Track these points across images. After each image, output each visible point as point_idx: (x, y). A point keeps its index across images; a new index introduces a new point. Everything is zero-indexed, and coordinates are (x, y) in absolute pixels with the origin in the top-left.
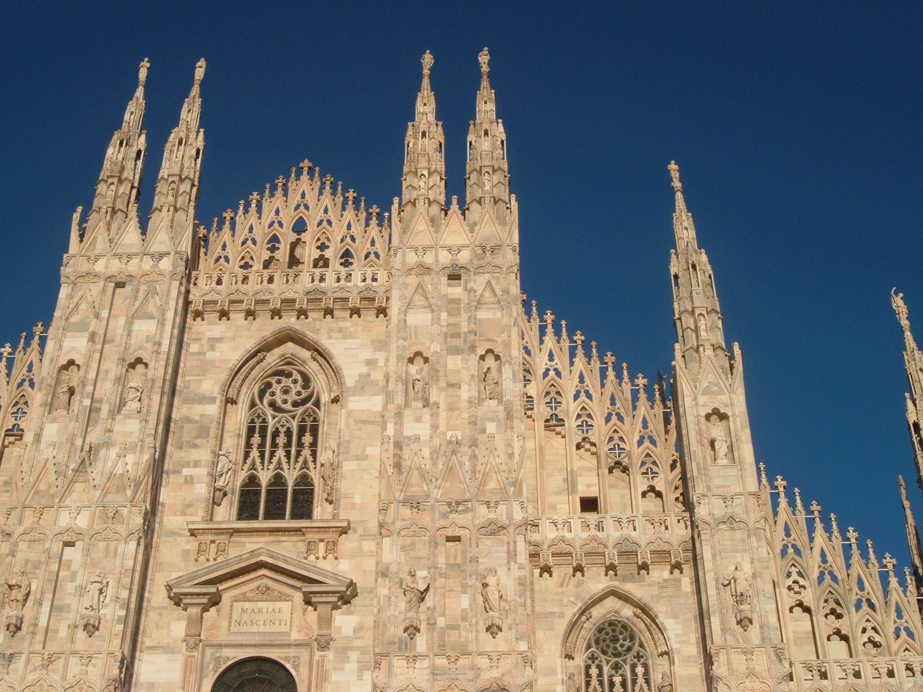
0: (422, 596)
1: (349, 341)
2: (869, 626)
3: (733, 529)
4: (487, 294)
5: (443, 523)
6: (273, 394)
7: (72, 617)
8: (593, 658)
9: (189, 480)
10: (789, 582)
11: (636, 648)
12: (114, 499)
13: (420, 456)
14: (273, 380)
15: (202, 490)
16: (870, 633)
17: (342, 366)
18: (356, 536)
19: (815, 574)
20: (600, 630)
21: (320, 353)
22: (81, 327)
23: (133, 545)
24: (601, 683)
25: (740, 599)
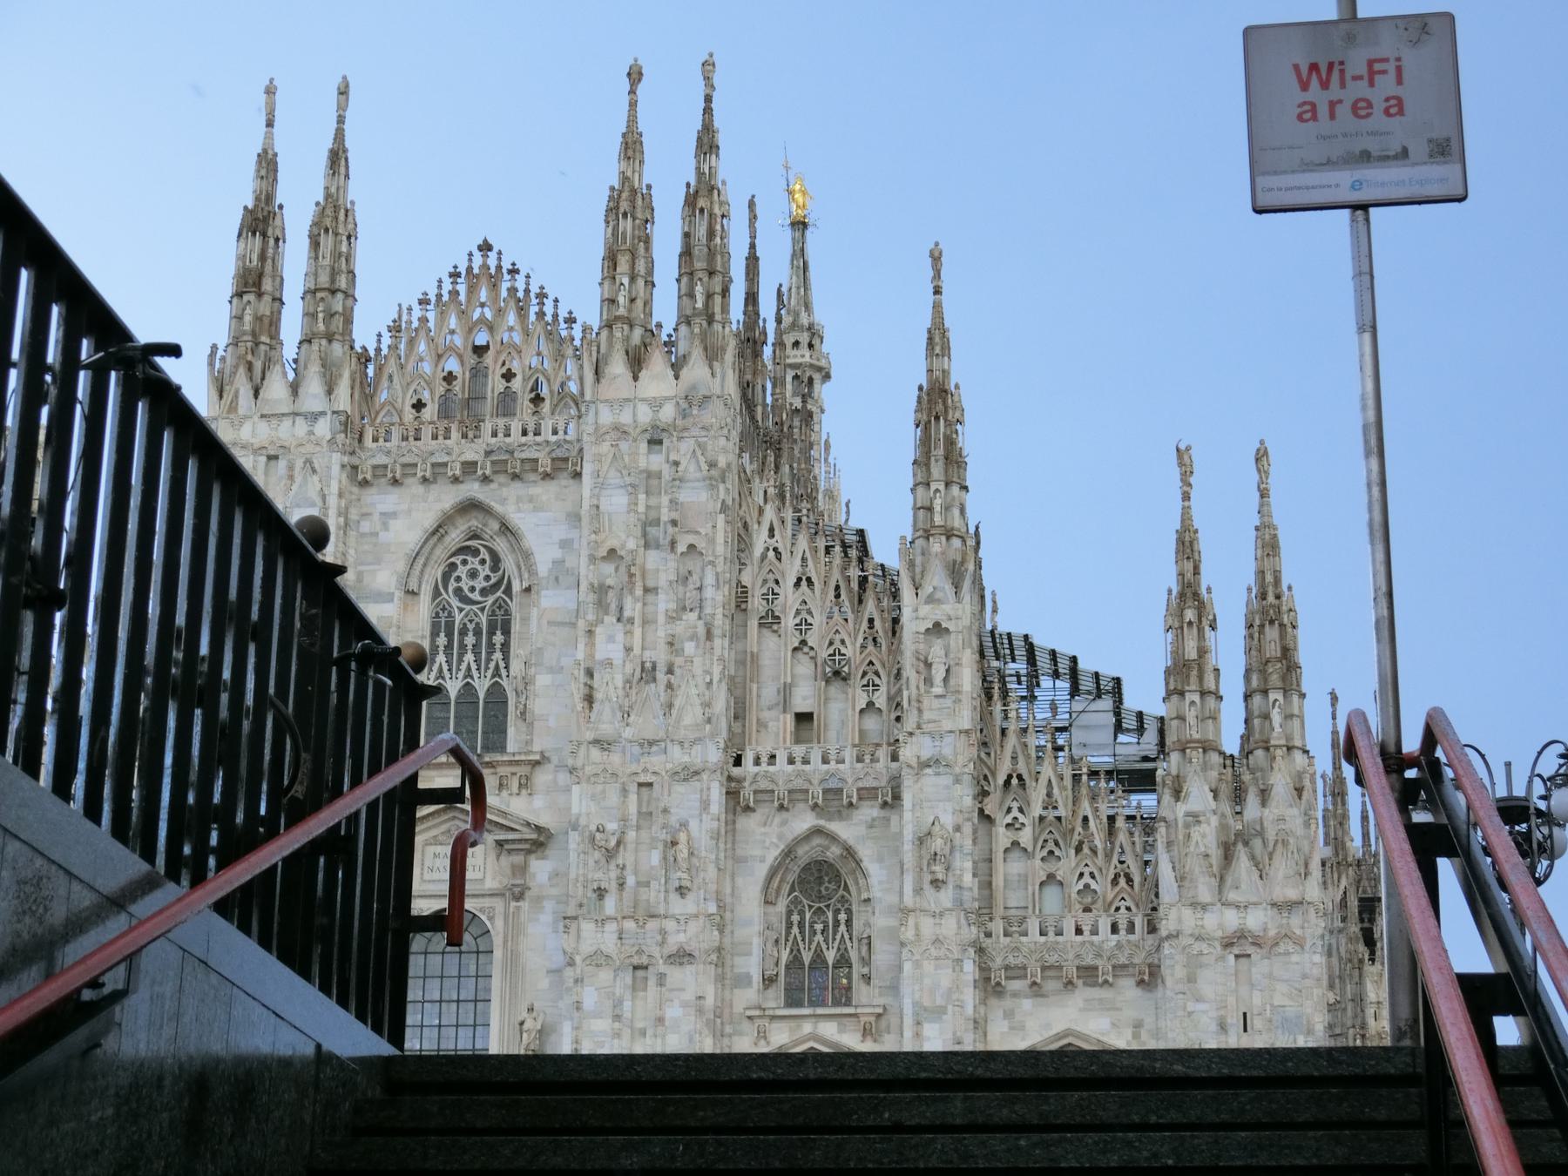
0: (610, 854)
1: (541, 514)
2: (1087, 871)
3: (938, 774)
4: (692, 468)
5: (634, 768)
6: (458, 579)
8: (796, 902)
10: (1009, 819)
11: (841, 892)
13: (610, 686)
14: (457, 560)
16: (1087, 879)
17: (535, 549)
18: (550, 767)
19: (1037, 810)
20: (806, 869)
21: (506, 529)
24: (802, 932)
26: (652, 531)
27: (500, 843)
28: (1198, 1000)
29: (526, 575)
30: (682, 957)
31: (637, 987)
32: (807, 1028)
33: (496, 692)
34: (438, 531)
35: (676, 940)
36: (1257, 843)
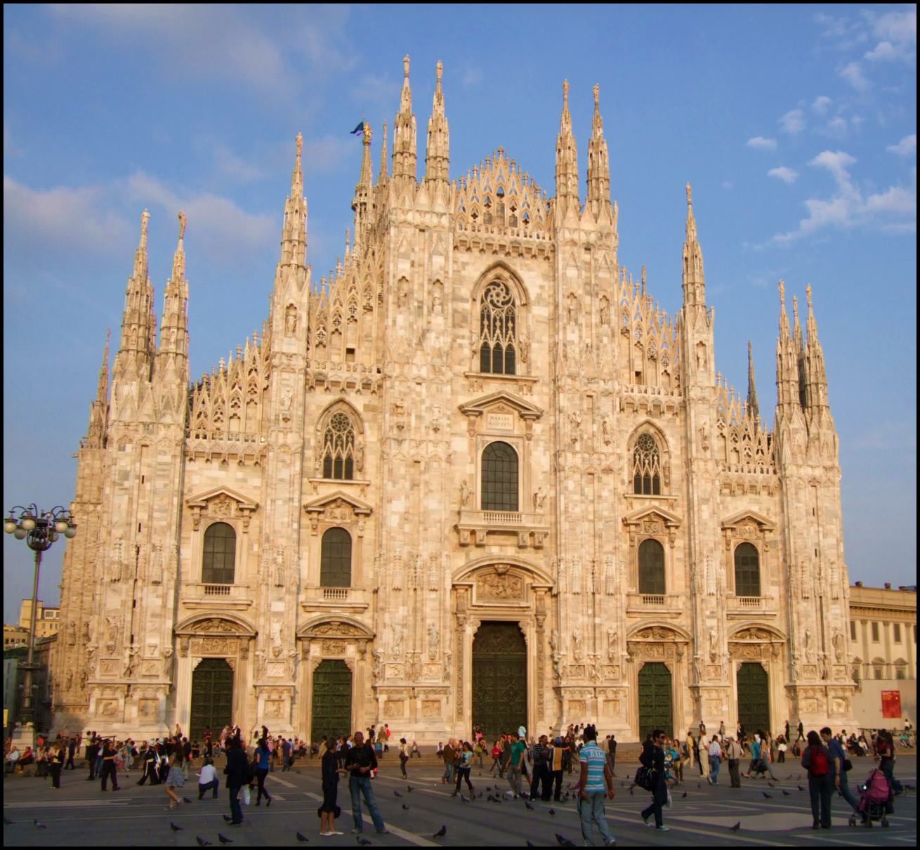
0: (578, 424)
1: (532, 274)
7: (427, 423)
8: (637, 450)
9: (461, 346)
12: (437, 362)
13: (574, 352)
14: (491, 287)
15: (467, 352)
20: (640, 438)
21: (514, 275)
22: (405, 256)
23: (449, 387)
25: (705, 438)
26: (588, 288)
28: (799, 501)
29: (524, 298)
30: (608, 471)
32: (647, 503)
33: (510, 347)
34: (484, 275)
35: (604, 463)
36: (817, 443)
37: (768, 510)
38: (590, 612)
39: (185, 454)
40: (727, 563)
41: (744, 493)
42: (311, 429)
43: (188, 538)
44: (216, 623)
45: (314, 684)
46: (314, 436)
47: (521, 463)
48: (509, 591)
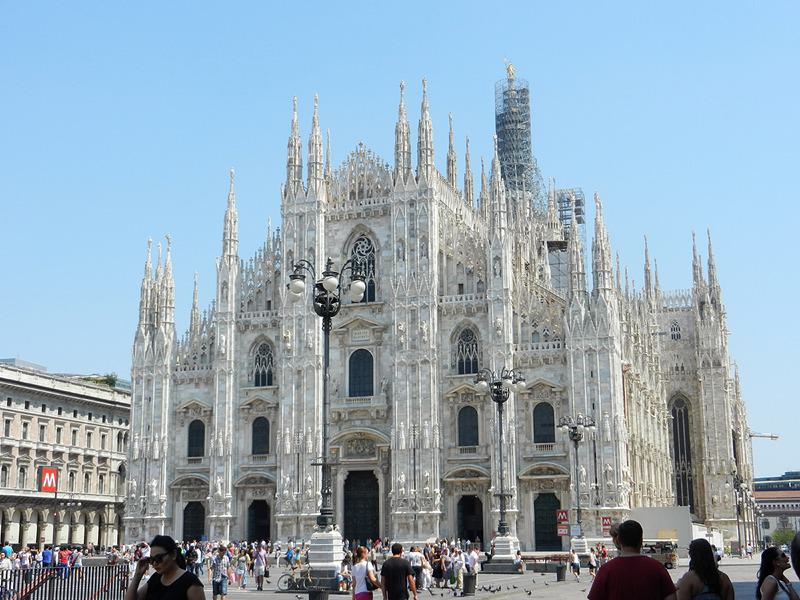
22: (290, 236)
25: (498, 329)
27: (373, 330)
30: (425, 362)
31: (414, 371)
32: (465, 381)
34: (352, 234)
37: (562, 376)
38: (412, 462)
39: (175, 381)
40: (527, 419)
41: (541, 365)
42: (245, 356)
43: (179, 431)
44: (193, 481)
45: (250, 515)
46: (247, 359)
47: (374, 362)
48: (367, 450)
